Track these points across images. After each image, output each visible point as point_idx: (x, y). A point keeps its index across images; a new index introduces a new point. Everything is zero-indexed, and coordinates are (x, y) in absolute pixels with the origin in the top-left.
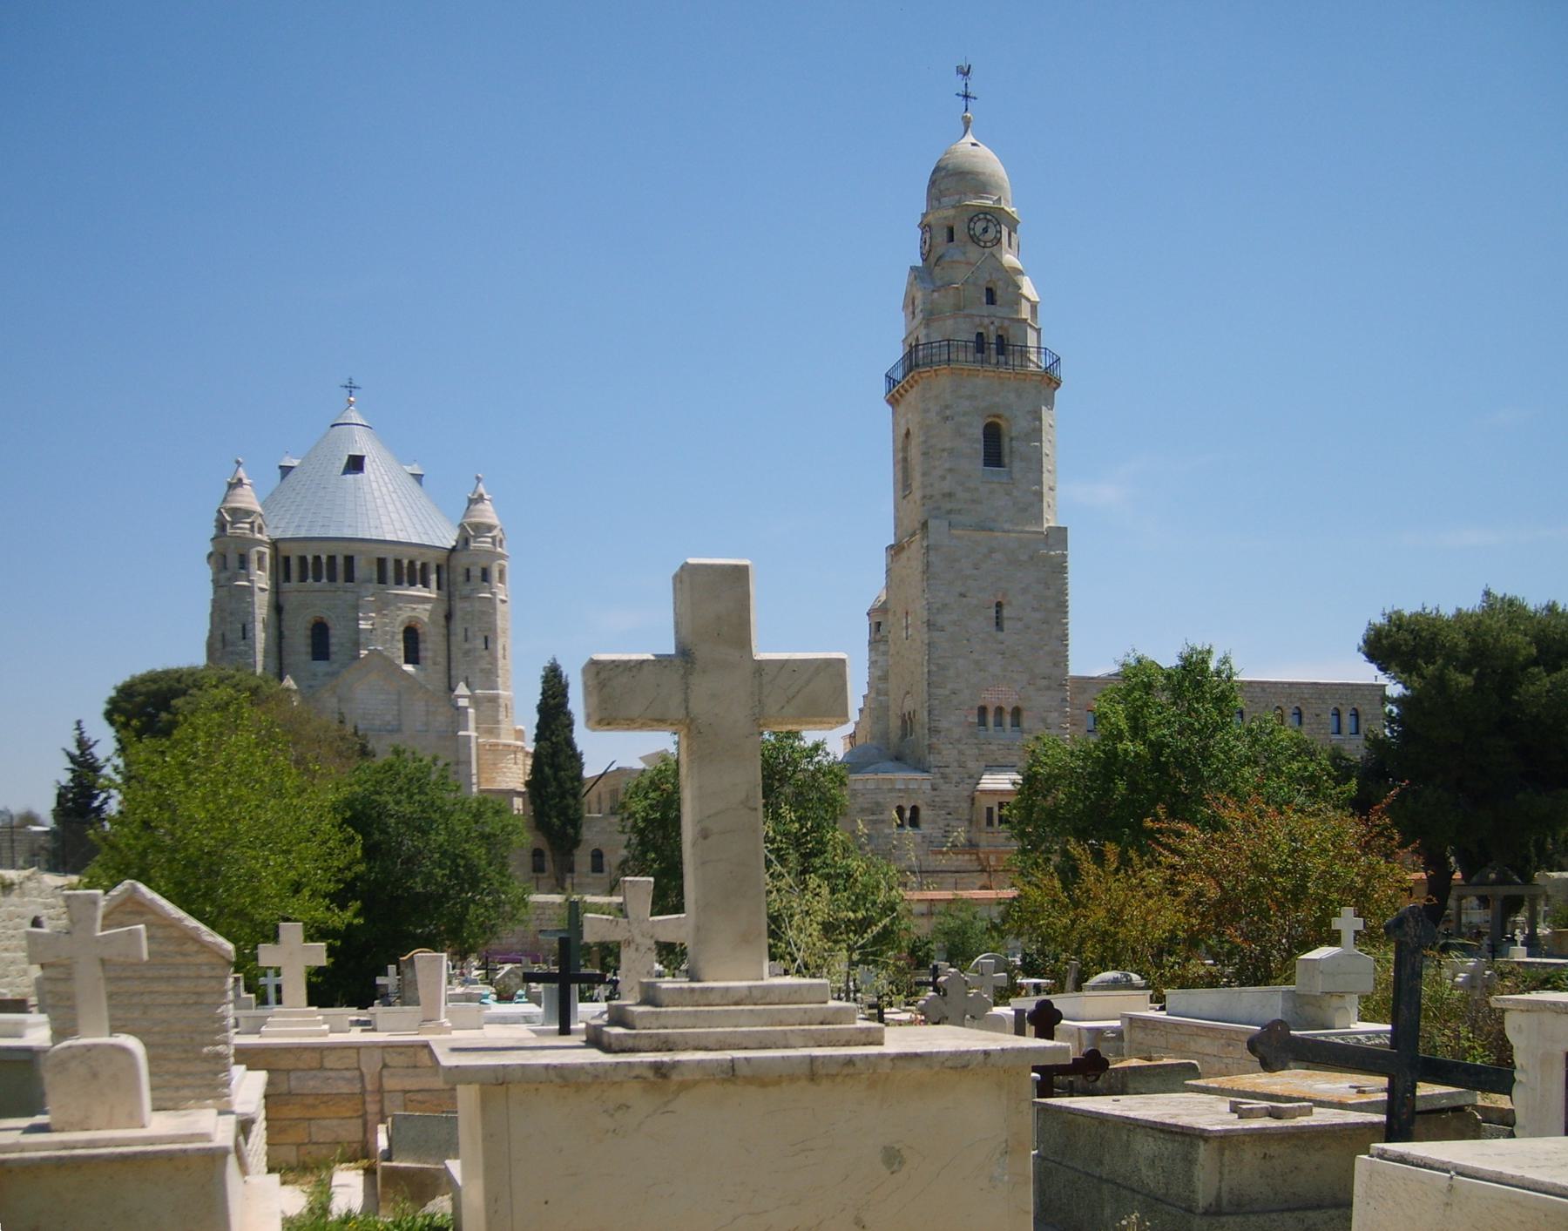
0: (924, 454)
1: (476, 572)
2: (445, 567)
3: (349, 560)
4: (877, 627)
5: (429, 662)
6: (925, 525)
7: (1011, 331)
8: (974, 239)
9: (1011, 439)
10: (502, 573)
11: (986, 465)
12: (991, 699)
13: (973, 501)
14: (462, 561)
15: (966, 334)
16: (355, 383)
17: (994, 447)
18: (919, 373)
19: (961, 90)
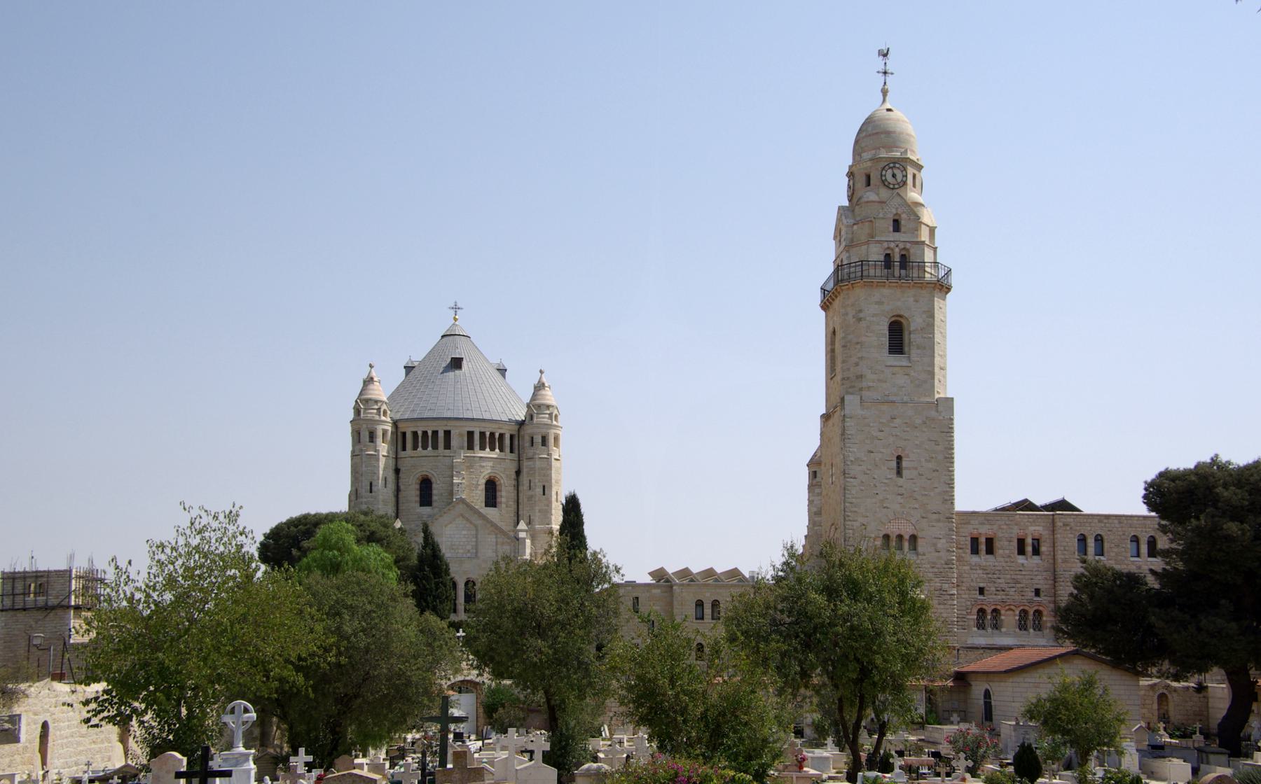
0: (844, 346)
1: (538, 439)
2: (517, 436)
3: (447, 433)
4: (813, 475)
5: (504, 506)
6: (843, 399)
7: (912, 251)
8: (884, 183)
9: (910, 334)
10: (556, 439)
11: (890, 352)
12: (893, 530)
13: (879, 380)
14: (528, 430)
15: (876, 254)
16: (459, 305)
17: (897, 338)
18: (840, 286)
19: (881, 68)
